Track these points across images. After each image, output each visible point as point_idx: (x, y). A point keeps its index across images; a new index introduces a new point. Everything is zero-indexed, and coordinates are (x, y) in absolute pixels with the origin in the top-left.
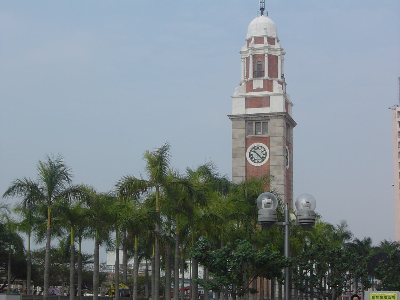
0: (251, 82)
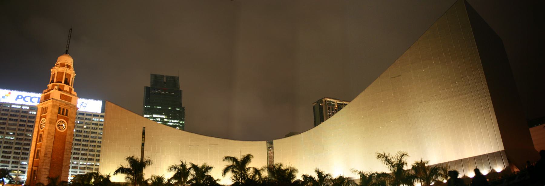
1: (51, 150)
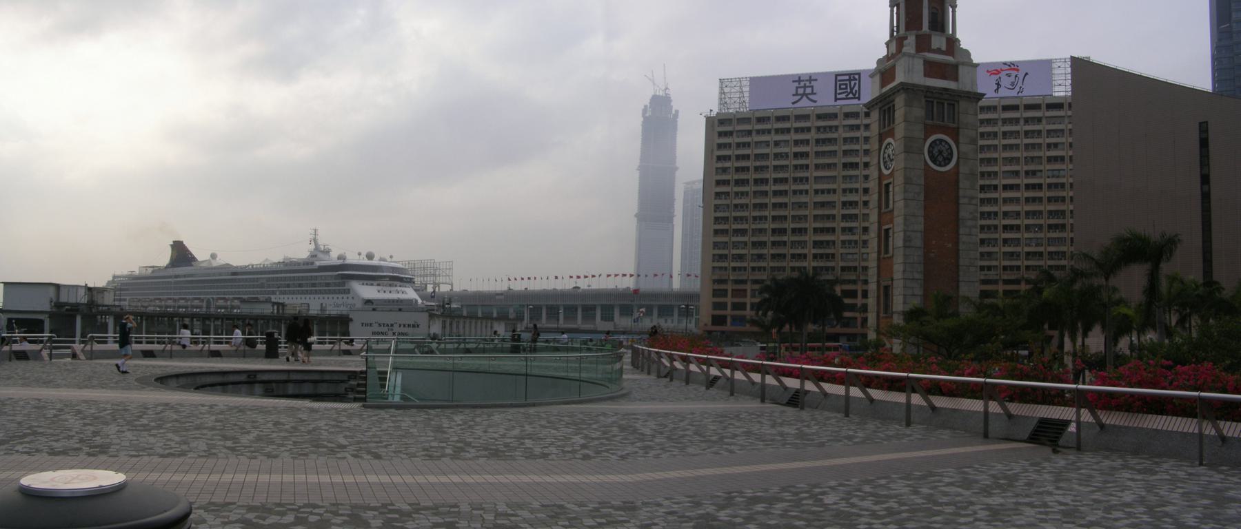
0: (929, 36)
1: (921, 227)
